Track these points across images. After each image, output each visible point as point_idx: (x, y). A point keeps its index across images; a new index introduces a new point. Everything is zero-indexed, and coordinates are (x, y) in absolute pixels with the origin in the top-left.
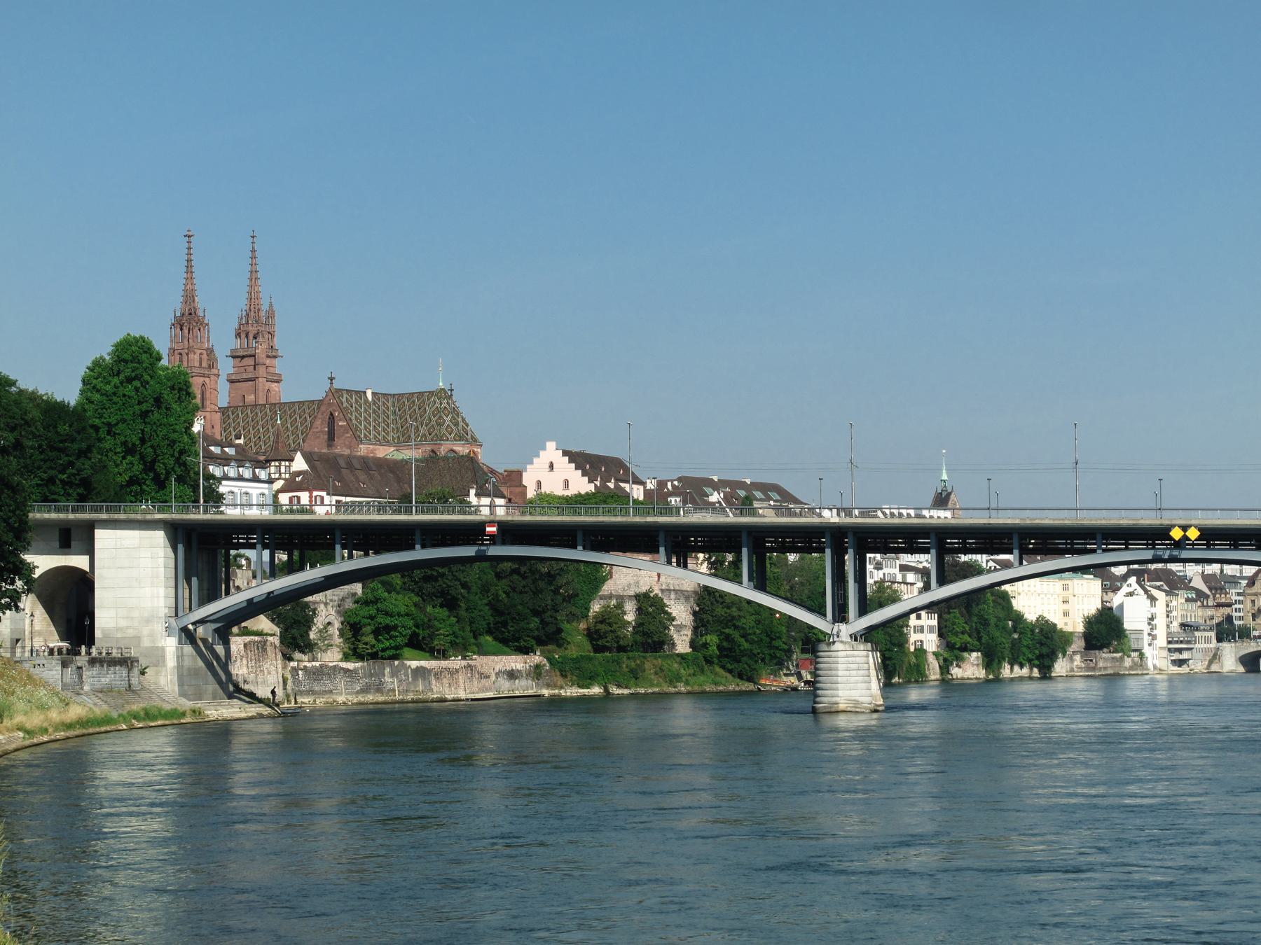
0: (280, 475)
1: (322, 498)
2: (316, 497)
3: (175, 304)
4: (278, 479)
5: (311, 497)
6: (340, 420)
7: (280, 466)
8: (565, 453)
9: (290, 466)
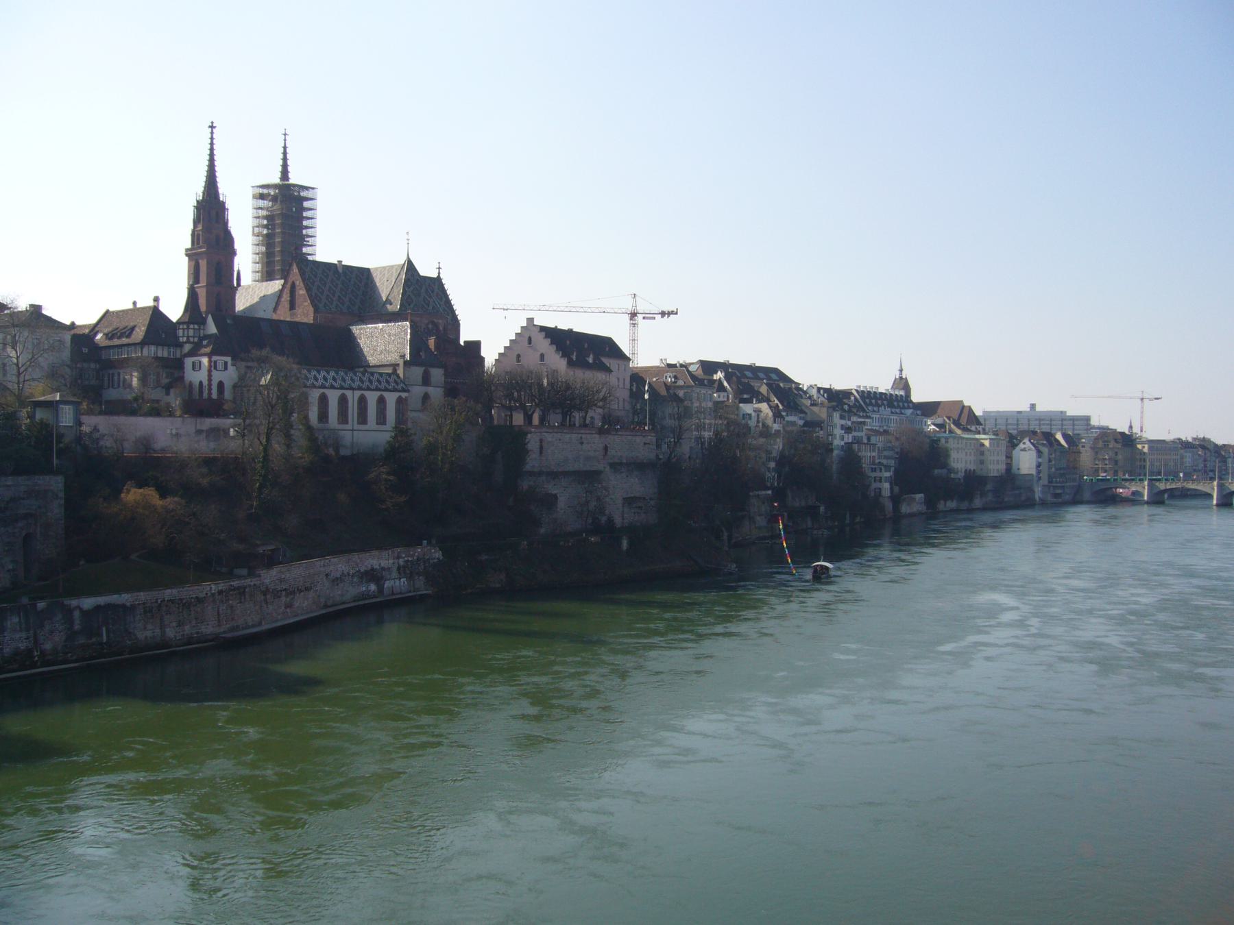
0: (188, 337)
1: (226, 363)
3: (197, 189)
4: (186, 343)
5: (210, 362)
6: (300, 289)
7: (188, 328)
9: (199, 329)
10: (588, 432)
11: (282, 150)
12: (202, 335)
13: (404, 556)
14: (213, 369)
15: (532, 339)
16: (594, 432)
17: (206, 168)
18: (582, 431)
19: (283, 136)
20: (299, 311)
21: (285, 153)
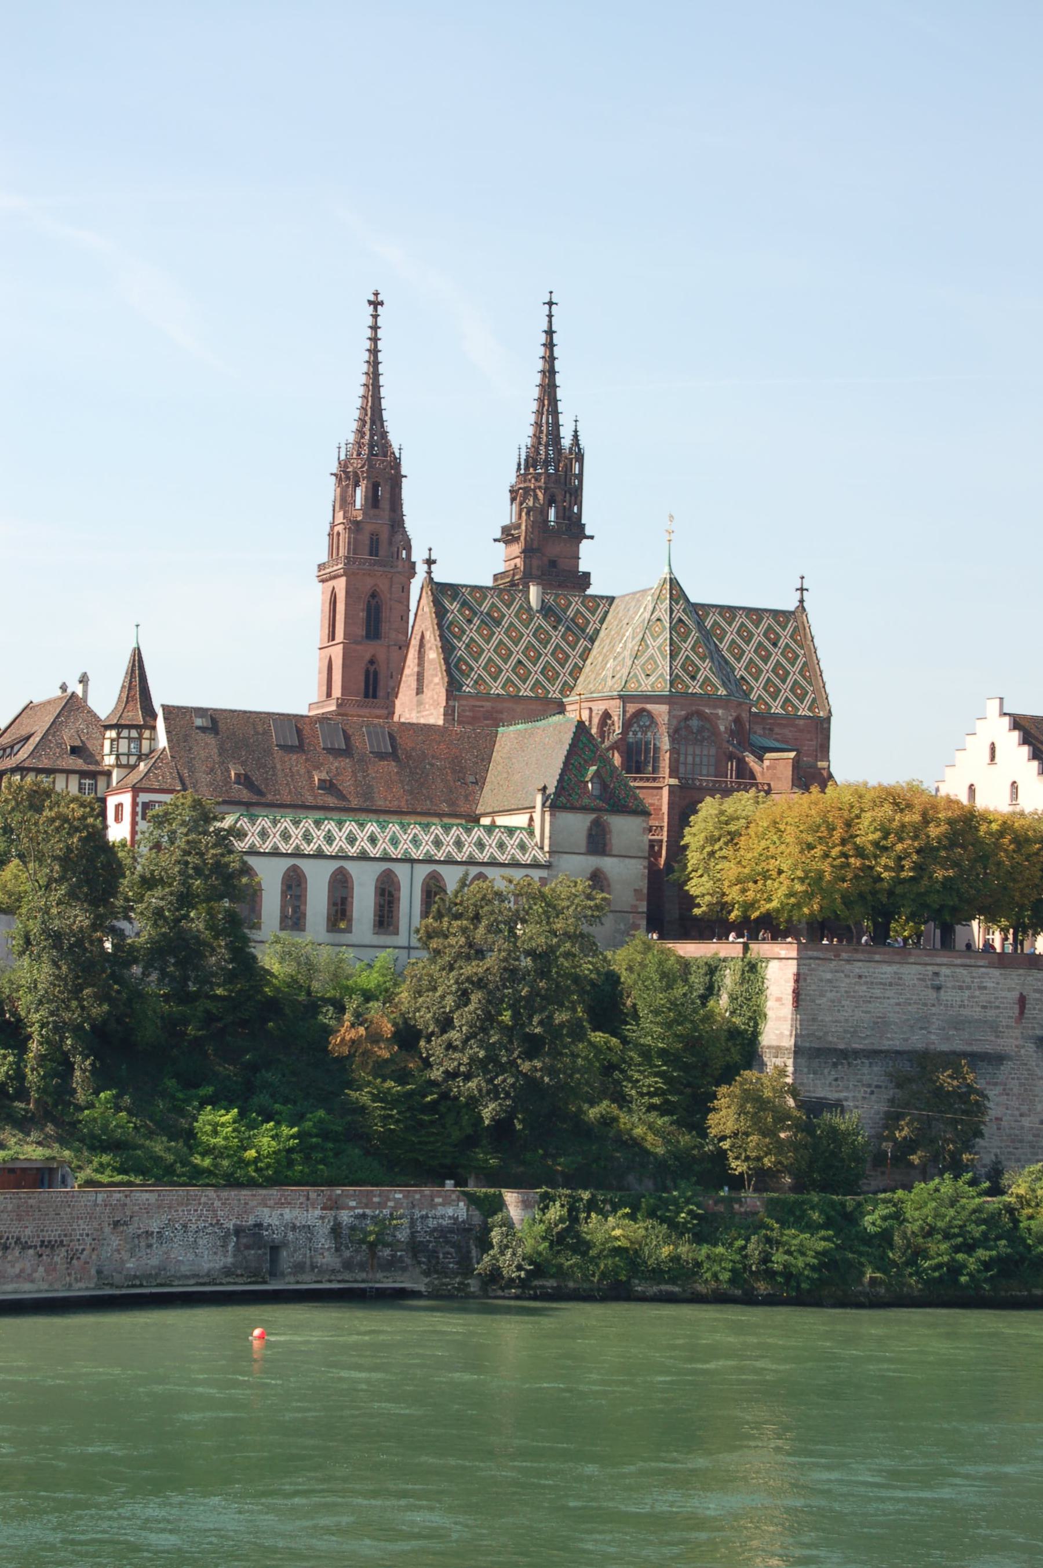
2: (146, 806)
5: (134, 804)
6: (431, 648)
8: (1018, 723)
9: (140, 738)
10: (959, 961)
11: (543, 338)
12: (145, 749)
13: (353, 1204)
14: (139, 818)
15: (996, 745)
16: (981, 963)
17: (361, 391)
18: (939, 960)
19: (547, 306)
20: (428, 693)
21: (550, 345)
